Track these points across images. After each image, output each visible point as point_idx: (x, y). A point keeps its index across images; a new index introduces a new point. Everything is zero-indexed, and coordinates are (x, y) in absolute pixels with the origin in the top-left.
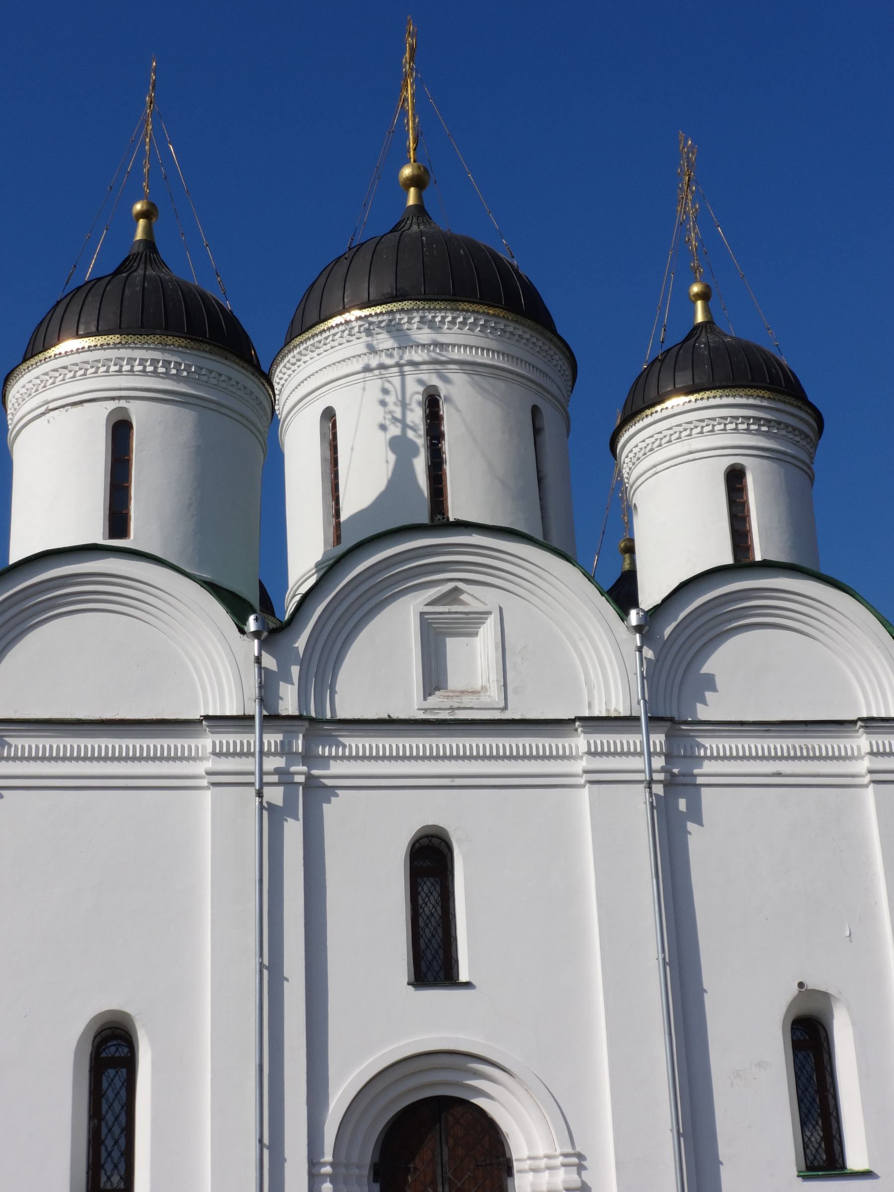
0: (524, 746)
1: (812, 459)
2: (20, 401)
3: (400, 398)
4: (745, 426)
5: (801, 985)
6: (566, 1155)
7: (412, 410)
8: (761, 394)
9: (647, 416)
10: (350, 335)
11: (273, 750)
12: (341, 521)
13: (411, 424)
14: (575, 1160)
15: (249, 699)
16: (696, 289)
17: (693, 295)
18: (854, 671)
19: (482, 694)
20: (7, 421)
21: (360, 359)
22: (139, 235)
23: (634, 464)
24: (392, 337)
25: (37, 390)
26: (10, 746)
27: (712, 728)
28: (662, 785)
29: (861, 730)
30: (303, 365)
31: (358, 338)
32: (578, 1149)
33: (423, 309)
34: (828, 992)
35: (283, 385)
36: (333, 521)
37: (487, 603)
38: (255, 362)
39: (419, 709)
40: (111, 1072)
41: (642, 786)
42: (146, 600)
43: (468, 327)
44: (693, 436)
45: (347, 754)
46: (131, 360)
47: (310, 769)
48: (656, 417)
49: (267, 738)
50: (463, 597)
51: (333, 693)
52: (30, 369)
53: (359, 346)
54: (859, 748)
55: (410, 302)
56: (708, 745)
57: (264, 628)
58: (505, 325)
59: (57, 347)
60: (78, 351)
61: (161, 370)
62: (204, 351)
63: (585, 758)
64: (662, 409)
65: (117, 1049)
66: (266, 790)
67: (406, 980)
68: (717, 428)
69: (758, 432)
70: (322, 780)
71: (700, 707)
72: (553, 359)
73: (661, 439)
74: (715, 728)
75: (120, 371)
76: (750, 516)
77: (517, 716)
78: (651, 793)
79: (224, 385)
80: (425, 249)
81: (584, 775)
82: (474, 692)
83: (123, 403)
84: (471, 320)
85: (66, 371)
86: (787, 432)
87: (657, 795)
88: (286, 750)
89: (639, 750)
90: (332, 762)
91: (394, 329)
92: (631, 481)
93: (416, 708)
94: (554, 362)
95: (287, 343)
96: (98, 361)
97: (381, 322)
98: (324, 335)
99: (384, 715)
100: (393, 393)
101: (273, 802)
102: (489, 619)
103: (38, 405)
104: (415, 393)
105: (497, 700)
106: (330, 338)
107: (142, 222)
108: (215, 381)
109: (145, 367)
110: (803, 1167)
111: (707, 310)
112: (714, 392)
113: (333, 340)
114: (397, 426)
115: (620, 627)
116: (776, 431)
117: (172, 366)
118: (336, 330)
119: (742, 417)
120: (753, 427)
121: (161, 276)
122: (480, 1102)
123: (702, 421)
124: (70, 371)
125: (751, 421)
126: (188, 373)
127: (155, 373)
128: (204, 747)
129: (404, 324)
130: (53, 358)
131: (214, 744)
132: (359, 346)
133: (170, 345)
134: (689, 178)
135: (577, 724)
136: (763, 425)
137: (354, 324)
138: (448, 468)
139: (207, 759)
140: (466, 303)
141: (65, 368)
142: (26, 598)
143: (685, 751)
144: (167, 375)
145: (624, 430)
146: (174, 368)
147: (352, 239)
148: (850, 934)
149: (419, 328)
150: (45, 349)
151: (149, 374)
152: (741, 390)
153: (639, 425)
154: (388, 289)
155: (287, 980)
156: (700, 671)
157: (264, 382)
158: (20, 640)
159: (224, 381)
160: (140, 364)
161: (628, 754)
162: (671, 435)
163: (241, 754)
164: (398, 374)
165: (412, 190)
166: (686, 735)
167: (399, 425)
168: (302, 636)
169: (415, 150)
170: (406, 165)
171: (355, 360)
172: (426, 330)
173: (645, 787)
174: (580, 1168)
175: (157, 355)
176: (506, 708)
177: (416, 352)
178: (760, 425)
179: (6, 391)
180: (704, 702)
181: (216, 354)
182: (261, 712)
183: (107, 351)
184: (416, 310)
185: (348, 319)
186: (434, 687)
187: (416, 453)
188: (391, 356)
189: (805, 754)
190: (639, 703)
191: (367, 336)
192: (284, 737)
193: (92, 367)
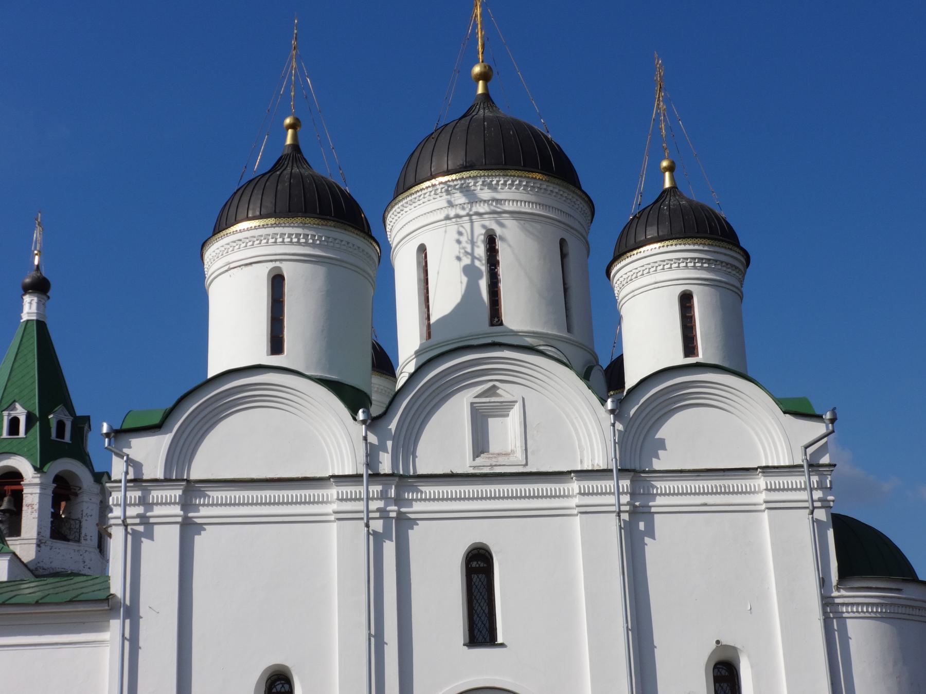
1: (742, 285)
3: (470, 238)
4: (692, 264)
5: (718, 642)
7: (478, 247)
8: (703, 242)
9: (628, 257)
10: (436, 194)
11: (375, 496)
12: (431, 323)
13: (477, 256)
15: (360, 463)
16: (665, 164)
17: (663, 169)
19: (512, 455)
20: (204, 272)
21: (442, 211)
22: (289, 141)
24: (464, 196)
25: (222, 255)
27: (661, 475)
28: (628, 514)
29: (760, 474)
30: (405, 214)
31: (441, 197)
33: (484, 176)
34: (736, 646)
35: (392, 226)
36: (426, 322)
38: (366, 230)
39: (471, 467)
41: (615, 514)
43: (514, 187)
44: (658, 271)
46: (282, 235)
47: (399, 508)
49: (371, 488)
51: (415, 457)
52: (218, 240)
53: (442, 201)
54: (759, 485)
55: (475, 171)
56: (659, 486)
57: (368, 418)
58: (541, 185)
59: (234, 226)
60: (248, 230)
61: (302, 241)
62: (330, 226)
64: (637, 253)
66: (371, 522)
67: (462, 642)
68: (674, 266)
69: (702, 268)
70: (408, 515)
71: (654, 460)
72: (575, 204)
73: (637, 273)
75: (275, 242)
76: (695, 325)
77: (534, 470)
79: (344, 248)
80: (486, 132)
81: (577, 508)
82: (506, 454)
83: (278, 264)
84: (517, 182)
85: (240, 242)
86: (722, 266)
87: (624, 521)
90: (414, 503)
91: (465, 190)
92: (620, 298)
93: (468, 466)
94: (577, 206)
95: (395, 198)
96: (261, 236)
97: (456, 185)
98: (419, 194)
99: (448, 471)
100: (465, 234)
103: (223, 265)
104: (480, 233)
106: (422, 196)
107: (290, 132)
108: (338, 246)
109: (292, 239)
111: (672, 179)
112: (671, 241)
113: (424, 198)
114: (468, 258)
115: (601, 411)
117: (309, 237)
118: (426, 191)
121: (302, 172)
123: (664, 261)
124: (243, 243)
125: (697, 261)
126: (320, 241)
127: (298, 243)
128: (332, 495)
129: (471, 186)
130: (232, 233)
131: (338, 493)
132: (442, 201)
133: (308, 224)
134: (660, 86)
135: (572, 474)
136: (705, 263)
137: (439, 187)
139: (334, 502)
140: (513, 171)
141: (240, 240)
142: (217, 401)
143: (643, 491)
144: (306, 244)
145: (614, 265)
146: (311, 239)
147: (437, 124)
148: (751, 608)
149: (481, 189)
150: (228, 226)
151: (295, 243)
152: (689, 240)
154: (460, 161)
155: (387, 644)
156: (655, 436)
157: (372, 241)
159: (344, 245)
160: (288, 237)
162: (643, 270)
163: (356, 499)
164: (469, 221)
165: (481, 83)
167: (470, 257)
168: (393, 421)
169: (482, 53)
170: (476, 65)
171: (438, 211)
173: (616, 516)
175: (299, 231)
176: (526, 464)
177: (480, 206)
178: (702, 263)
179: (203, 253)
180: (658, 457)
181: (338, 228)
182: (367, 472)
183: (267, 229)
184: (479, 177)
185: (434, 184)
186: (480, 451)
187: (481, 277)
188: (463, 209)
189: (723, 490)
190: (612, 460)
191: (447, 195)
193: (257, 240)
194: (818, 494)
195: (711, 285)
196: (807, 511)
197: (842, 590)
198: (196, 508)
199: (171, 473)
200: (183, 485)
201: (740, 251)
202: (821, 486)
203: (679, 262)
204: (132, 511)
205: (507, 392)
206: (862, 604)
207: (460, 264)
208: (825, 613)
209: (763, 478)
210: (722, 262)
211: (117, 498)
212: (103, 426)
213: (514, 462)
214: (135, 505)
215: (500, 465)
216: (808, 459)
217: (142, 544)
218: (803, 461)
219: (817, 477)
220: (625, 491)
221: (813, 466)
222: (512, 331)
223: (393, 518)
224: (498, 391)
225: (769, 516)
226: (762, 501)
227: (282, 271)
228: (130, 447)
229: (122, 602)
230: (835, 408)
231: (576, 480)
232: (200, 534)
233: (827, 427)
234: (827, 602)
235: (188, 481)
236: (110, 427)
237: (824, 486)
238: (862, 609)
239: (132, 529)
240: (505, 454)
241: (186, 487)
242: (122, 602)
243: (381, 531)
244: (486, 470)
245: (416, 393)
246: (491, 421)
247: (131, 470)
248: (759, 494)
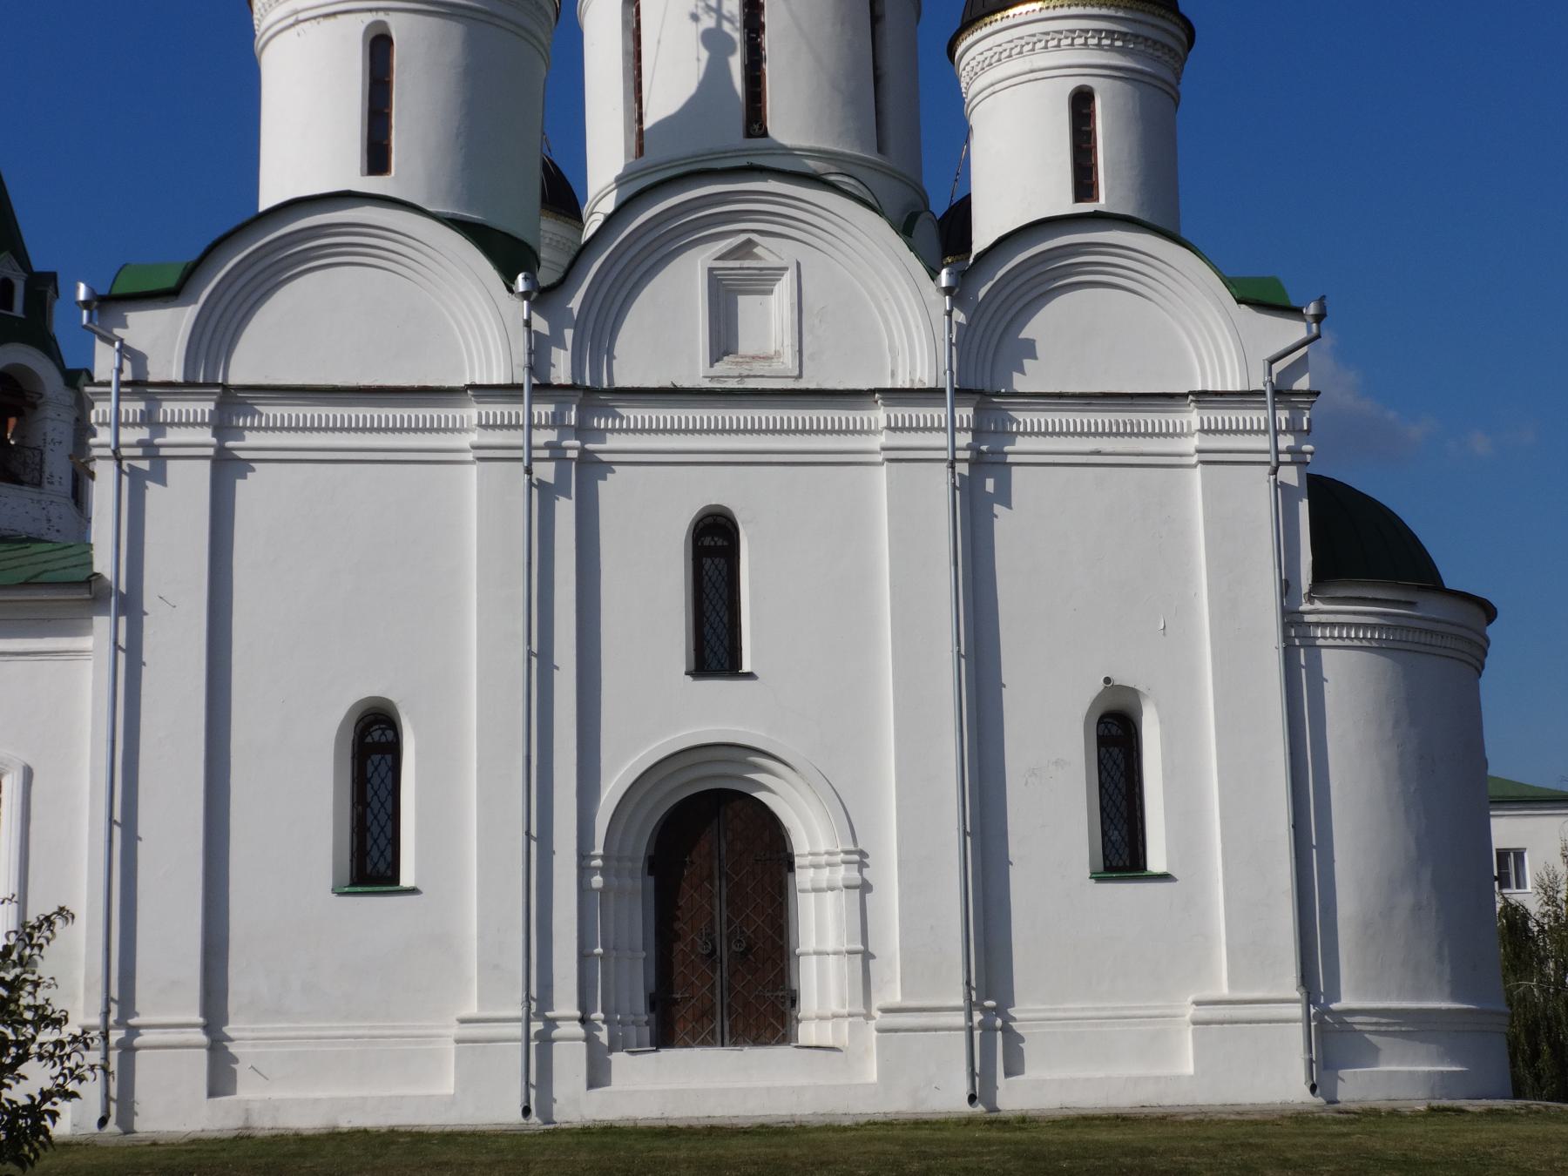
0: (818, 420)
1: (1178, 79)
2: (267, 6)
4: (1095, 41)
5: (1107, 680)
6: (847, 852)
9: (986, 25)
11: (543, 422)
12: (644, 129)
14: (856, 857)
15: (518, 365)
19: (775, 360)
20: (253, 25)
23: (971, 79)
27: (1026, 400)
29: (1192, 405)
32: (860, 846)
37: (783, 257)
40: (376, 758)
41: (945, 465)
42: (409, 255)
45: (625, 426)
47: (584, 442)
48: (996, 26)
49: (536, 409)
51: (611, 358)
54: (1189, 424)
56: (1021, 420)
63: (884, 433)
64: (1002, 19)
65: (383, 733)
66: (535, 466)
67: (684, 669)
68: (1064, 42)
69: (1112, 48)
70: (597, 455)
71: (1016, 376)
73: (1001, 53)
74: (1030, 401)
77: (813, 386)
78: (953, 473)
81: (883, 452)
82: (767, 358)
83: (381, 16)
86: (1145, 46)
88: (558, 423)
89: (943, 425)
90: (608, 435)
92: (970, 97)
93: (701, 375)
99: (667, 384)
101: (544, 479)
102: (785, 276)
105: (790, 367)
110: (1100, 867)
114: (711, 17)
115: (929, 288)
116: (1132, 46)
119: (1093, 30)
120: (1106, 42)
123: (1047, 33)
125: (1103, 35)
128: (469, 418)
135: (877, 395)
136: (1117, 39)
138: (767, 67)
139: (473, 431)
145: (961, 39)
148: (1165, 627)
153: (978, 34)
155: (557, 668)
158: (272, 295)
161: (931, 429)
162: (1012, 49)
163: (510, 427)
166: (998, 408)
174: (862, 865)
176: (800, 376)
178: (1113, 40)
180: (1022, 371)
186: (722, 351)
187: (732, 51)
189: (1129, 430)
190: (945, 373)
192: (556, 408)
194: (1286, 441)
195: (1127, 79)
196: (1267, 469)
197: (1316, 601)
198: (238, 433)
199: (196, 373)
200: (215, 393)
201: (1178, 21)
202: (1293, 428)
203: (1073, 35)
204: (129, 436)
205: (770, 252)
206: (1349, 625)
207: (697, 27)
208: (1286, 638)
209: (1196, 410)
210: (1146, 39)
211: (104, 412)
212: (78, 288)
213: (780, 372)
214: (134, 425)
215: (755, 376)
216: (1274, 381)
217: (147, 491)
218: (1265, 385)
219: (1287, 412)
220: (965, 425)
221: (1282, 394)
222: (783, 147)
223: (571, 459)
224: (755, 250)
225: (1203, 475)
226: (1192, 450)
227: (388, 29)
228: (125, 326)
229: (113, 587)
230: (1324, 296)
231: (882, 404)
233: (1309, 330)
234: (1291, 620)
235: (225, 387)
236: (91, 290)
237: (1297, 428)
238: (1348, 633)
239: (129, 465)
240: (763, 358)
241: (221, 397)
242: (113, 587)
243: (552, 481)
244: (732, 384)
245: (617, 246)
246: (743, 301)
247: (127, 365)
248: (1189, 437)
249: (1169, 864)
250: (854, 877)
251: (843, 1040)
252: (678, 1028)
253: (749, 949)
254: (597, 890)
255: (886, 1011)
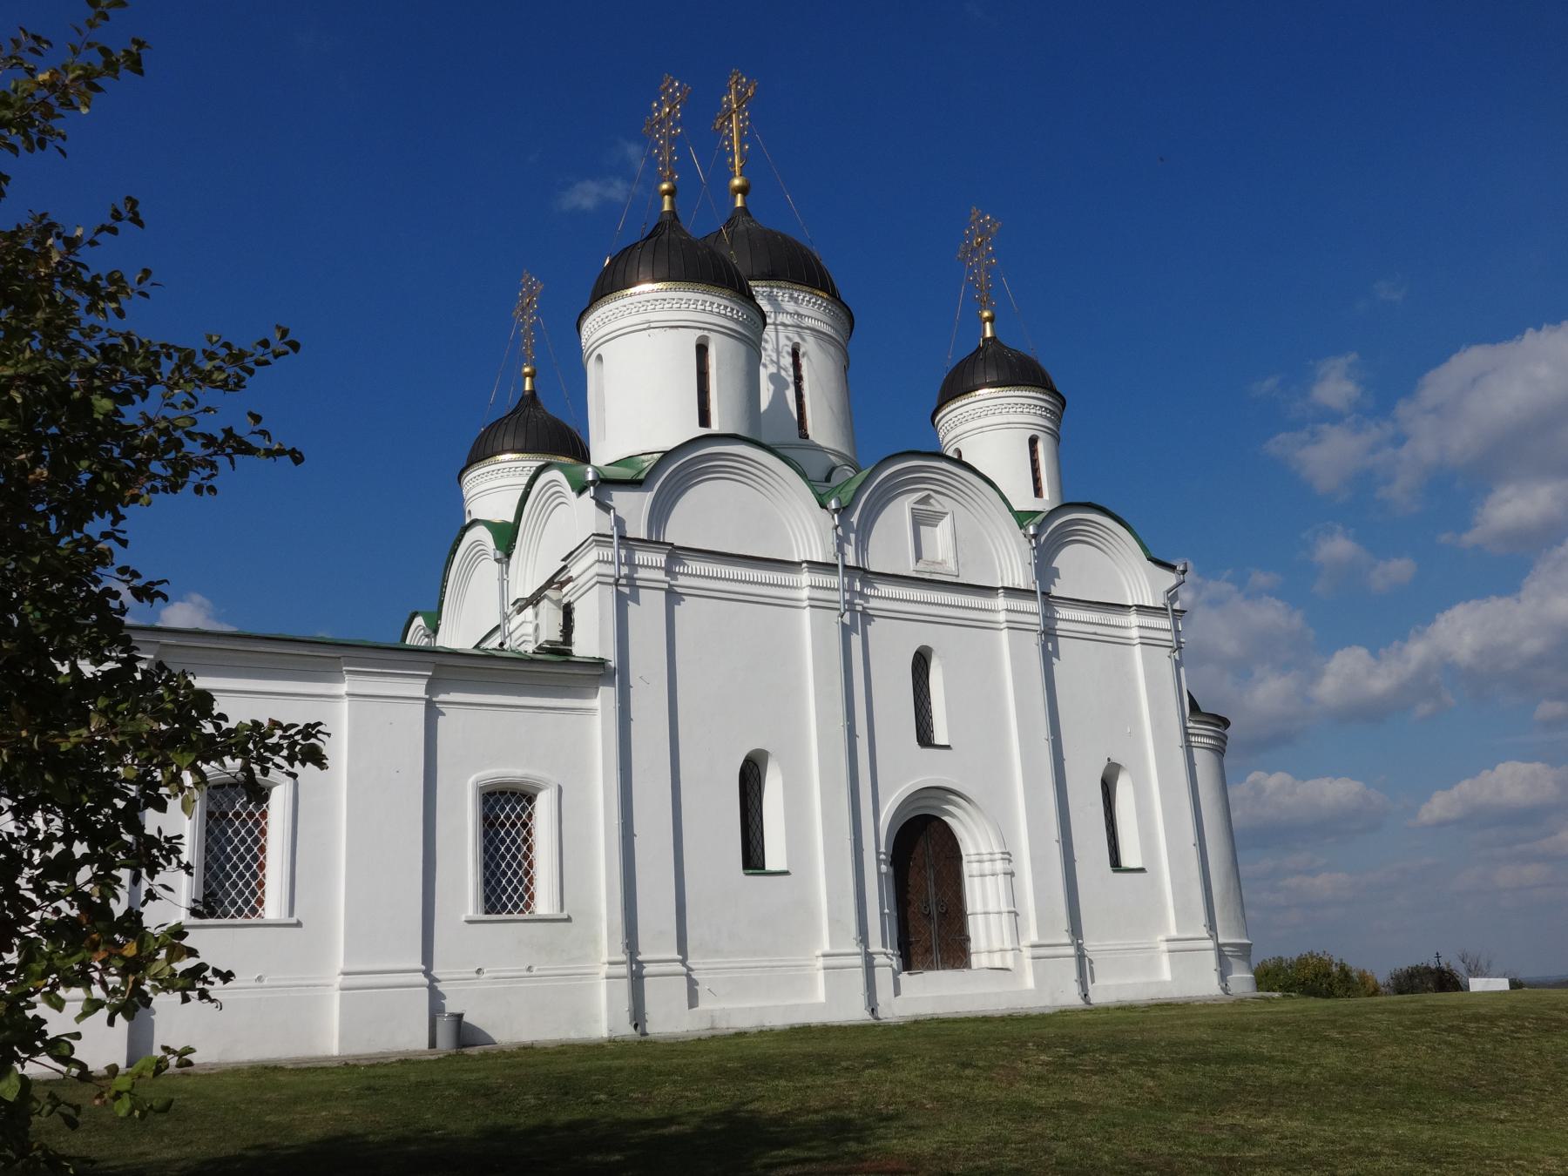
3: (775, 347)
5: (1109, 759)
6: (1003, 853)
7: (784, 357)
18: (1124, 574)
22: (666, 208)
24: (770, 304)
26: (688, 567)
33: (792, 288)
50: (932, 501)
69: (1046, 417)
83: (706, 333)
90: (870, 599)
96: (690, 300)
97: (764, 292)
100: (771, 342)
122: (946, 818)
123: (1017, 404)
124: (668, 303)
135: (999, 591)
141: (665, 300)
144: (731, 318)
149: (789, 301)
163: (833, 589)
167: (776, 366)
172: (792, 303)
174: (1010, 861)
176: (958, 576)
187: (787, 387)
200: (667, 549)
205: (938, 503)
232: (680, 605)
244: (927, 576)
249: (1143, 864)
250: (1009, 867)
251: (1010, 963)
252: (914, 959)
253: (946, 912)
254: (885, 874)
255: (1033, 946)
